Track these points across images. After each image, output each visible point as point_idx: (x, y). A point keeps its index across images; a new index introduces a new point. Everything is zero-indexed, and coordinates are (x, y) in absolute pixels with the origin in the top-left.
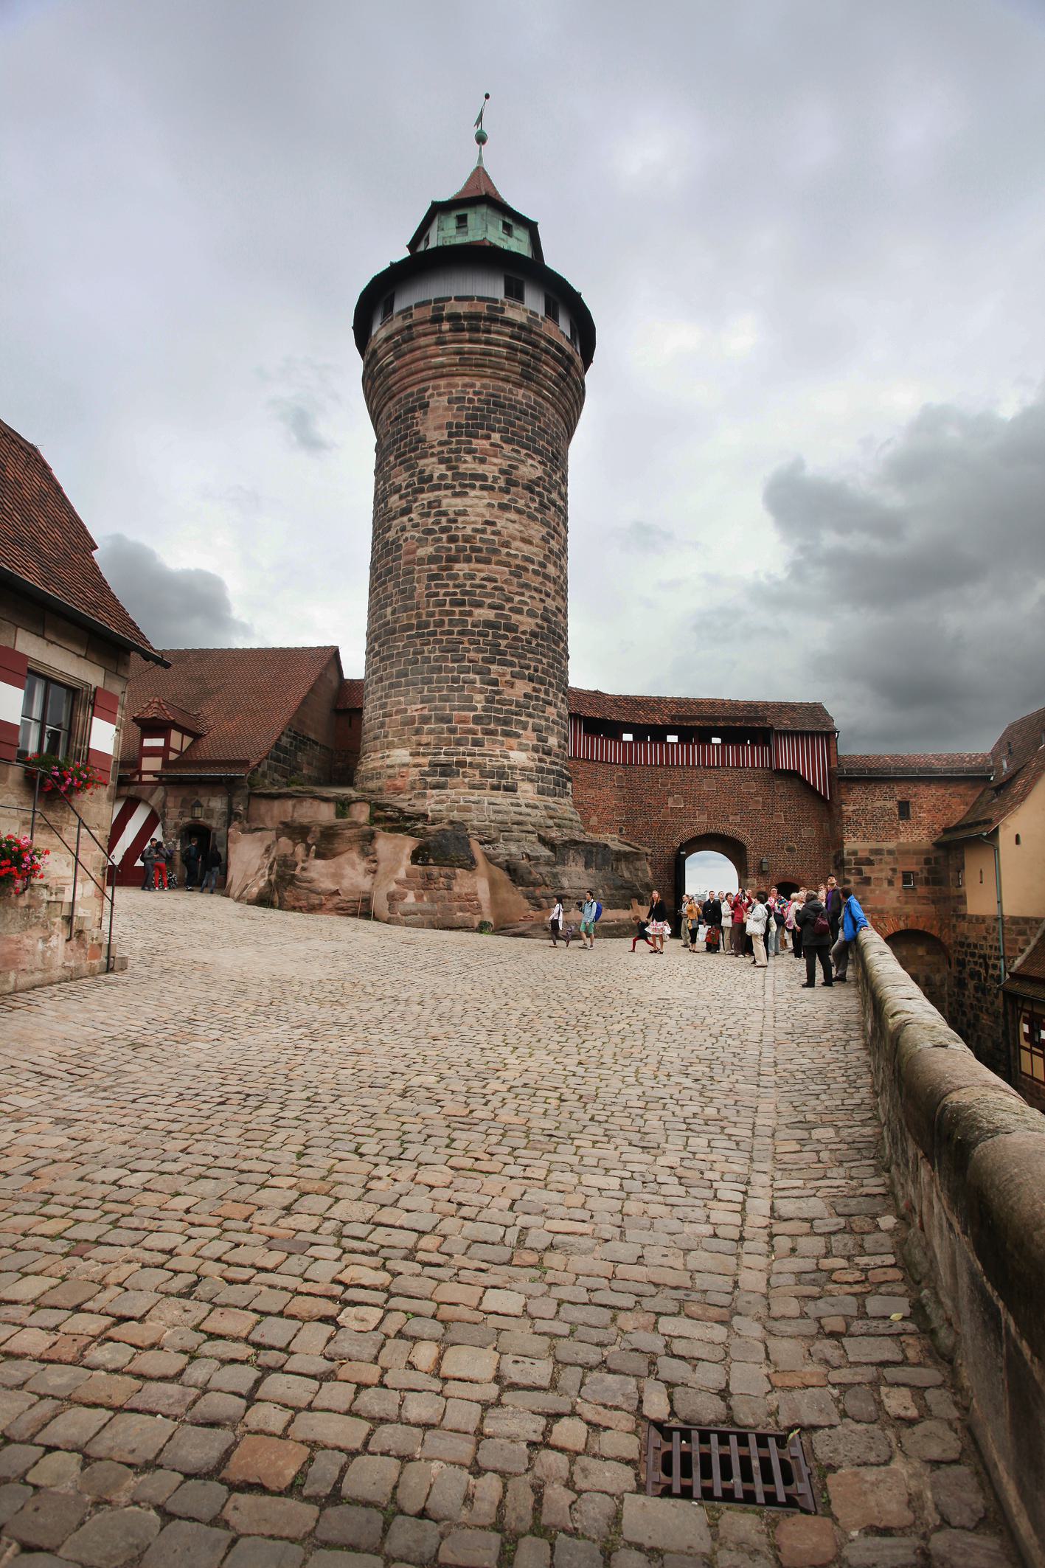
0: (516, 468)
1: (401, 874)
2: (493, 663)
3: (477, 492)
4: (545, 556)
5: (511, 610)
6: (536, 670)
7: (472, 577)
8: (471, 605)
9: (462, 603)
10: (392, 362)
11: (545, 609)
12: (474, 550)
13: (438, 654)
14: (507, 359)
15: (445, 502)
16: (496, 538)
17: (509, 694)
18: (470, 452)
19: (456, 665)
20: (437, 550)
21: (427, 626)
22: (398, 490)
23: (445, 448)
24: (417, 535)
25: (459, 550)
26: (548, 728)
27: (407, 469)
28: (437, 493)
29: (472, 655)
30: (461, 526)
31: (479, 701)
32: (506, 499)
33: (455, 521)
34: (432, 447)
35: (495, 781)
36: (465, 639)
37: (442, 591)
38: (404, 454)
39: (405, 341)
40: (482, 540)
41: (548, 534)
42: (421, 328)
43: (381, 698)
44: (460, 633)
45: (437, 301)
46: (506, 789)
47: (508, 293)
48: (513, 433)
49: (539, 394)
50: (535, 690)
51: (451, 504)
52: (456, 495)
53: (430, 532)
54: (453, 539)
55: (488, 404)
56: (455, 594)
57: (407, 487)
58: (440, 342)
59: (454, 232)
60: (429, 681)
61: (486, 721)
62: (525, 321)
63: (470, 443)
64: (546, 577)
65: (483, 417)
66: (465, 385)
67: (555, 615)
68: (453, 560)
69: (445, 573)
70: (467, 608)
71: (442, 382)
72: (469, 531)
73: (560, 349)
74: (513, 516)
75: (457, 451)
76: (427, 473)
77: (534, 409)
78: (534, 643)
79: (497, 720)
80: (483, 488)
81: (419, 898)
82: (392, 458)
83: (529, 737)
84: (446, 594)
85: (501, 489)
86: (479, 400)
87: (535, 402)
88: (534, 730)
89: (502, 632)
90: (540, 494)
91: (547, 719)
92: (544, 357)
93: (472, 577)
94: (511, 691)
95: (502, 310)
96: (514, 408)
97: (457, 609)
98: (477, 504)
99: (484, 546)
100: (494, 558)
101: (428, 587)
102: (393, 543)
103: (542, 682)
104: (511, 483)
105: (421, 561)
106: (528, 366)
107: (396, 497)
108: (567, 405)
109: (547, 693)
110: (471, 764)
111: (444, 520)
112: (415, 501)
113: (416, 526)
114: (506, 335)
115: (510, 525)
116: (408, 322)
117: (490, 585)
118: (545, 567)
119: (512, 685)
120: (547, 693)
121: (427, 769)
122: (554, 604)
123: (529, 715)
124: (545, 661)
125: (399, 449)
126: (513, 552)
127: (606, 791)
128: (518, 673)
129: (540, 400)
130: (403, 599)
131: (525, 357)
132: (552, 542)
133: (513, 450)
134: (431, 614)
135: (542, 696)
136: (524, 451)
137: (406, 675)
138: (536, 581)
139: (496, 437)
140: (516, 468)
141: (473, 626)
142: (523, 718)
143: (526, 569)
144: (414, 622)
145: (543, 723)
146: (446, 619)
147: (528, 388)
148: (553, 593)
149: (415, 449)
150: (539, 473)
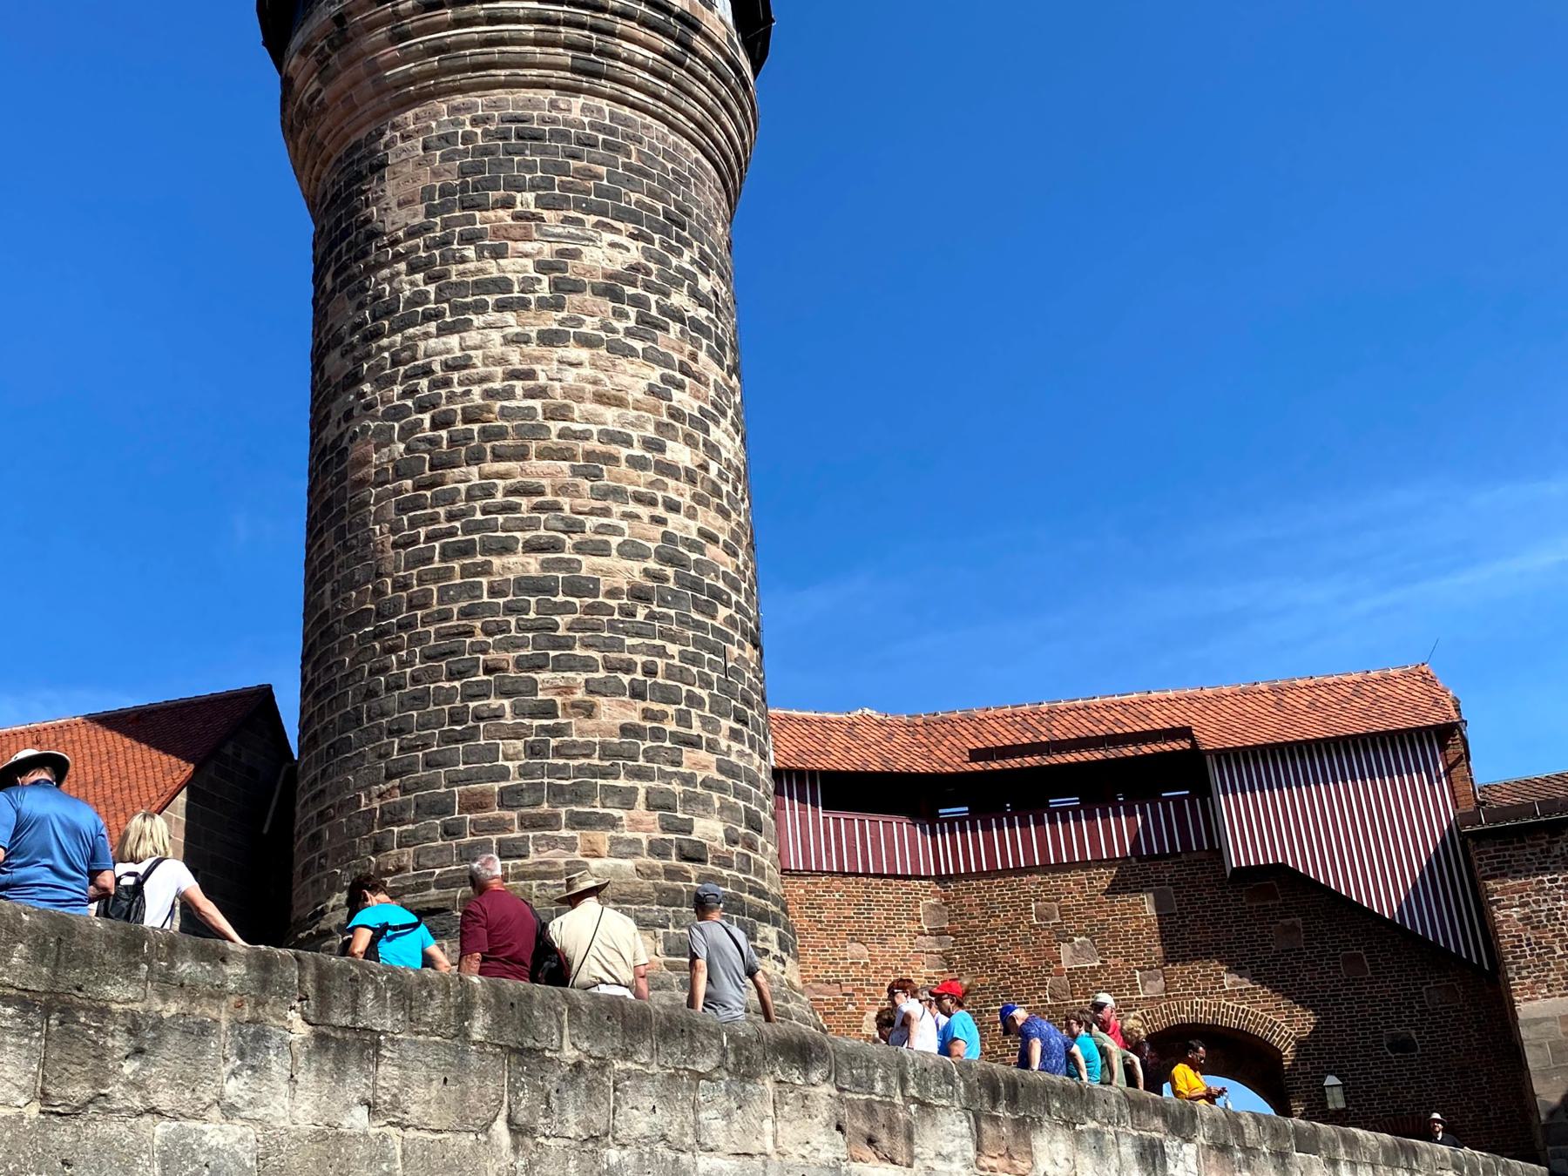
0: (576, 255)
2: (540, 667)
3: (492, 316)
4: (659, 426)
5: (578, 548)
6: (650, 671)
8: (487, 551)
9: (466, 550)
10: (319, 91)
14: (536, 43)
15: (422, 345)
16: (537, 404)
17: (580, 730)
19: (457, 684)
25: (452, 441)
26: (690, 799)
29: (493, 654)
30: (458, 390)
31: (512, 755)
32: (551, 320)
33: (447, 383)
34: (395, 242)
38: (345, 267)
39: (334, 48)
40: (505, 413)
43: (315, 780)
44: (465, 613)
48: (564, 187)
50: (647, 714)
52: (444, 330)
53: (398, 413)
55: (505, 138)
56: (451, 533)
63: (471, 220)
64: (669, 469)
65: (500, 164)
67: (700, 549)
70: (479, 558)
74: (574, 352)
75: (445, 242)
77: (613, 132)
79: (557, 793)
80: (501, 307)
83: (642, 825)
85: (543, 304)
86: (486, 133)
87: (613, 116)
88: (650, 807)
89: (560, 598)
90: (637, 301)
91: (688, 780)
92: (621, 25)
93: (488, 492)
94: (588, 724)
96: (565, 136)
100: (533, 445)
103: (669, 696)
106: (588, 49)
108: (698, 111)
109: (683, 718)
111: (424, 383)
115: (570, 375)
117: (524, 502)
118: (661, 448)
119: (589, 711)
120: (683, 718)
122: (693, 526)
126: (575, 427)
127: (901, 943)
128: (604, 682)
129: (627, 111)
131: (574, 34)
132: (676, 394)
133: (566, 220)
135: (670, 726)
138: (641, 480)
139: (526, 200)
140: (576, 255)
141: (493, 592)
142: (622, 782)
143: (612, 459)
145: (677, 787)
148: (686, 501)
150: (635, 253)
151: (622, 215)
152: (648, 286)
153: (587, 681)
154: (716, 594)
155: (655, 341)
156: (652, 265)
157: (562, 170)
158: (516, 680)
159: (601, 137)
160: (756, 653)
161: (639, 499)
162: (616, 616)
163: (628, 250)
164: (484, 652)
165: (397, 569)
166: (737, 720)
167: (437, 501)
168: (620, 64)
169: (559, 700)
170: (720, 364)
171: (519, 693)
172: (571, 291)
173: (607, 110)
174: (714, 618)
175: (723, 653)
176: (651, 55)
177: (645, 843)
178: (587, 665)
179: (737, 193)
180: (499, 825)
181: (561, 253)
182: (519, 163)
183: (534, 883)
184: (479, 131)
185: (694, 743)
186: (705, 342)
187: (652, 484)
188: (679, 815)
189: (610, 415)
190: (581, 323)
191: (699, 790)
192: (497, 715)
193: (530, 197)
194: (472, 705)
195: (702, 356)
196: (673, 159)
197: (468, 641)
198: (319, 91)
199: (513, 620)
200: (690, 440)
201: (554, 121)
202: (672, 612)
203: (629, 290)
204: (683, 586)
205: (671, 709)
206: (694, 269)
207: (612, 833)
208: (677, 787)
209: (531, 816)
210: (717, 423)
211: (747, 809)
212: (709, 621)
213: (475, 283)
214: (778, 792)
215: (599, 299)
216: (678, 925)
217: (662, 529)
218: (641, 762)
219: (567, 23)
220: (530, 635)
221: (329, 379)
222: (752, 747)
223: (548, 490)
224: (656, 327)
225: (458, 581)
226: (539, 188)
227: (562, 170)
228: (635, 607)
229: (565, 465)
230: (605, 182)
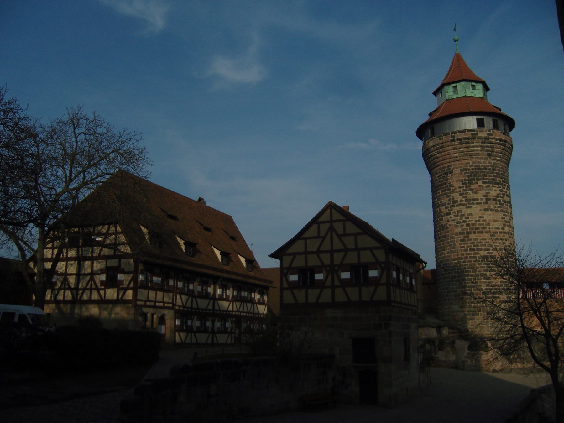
0: (489, 193)
1: (465, 354)
7: (477, 239)
9: (474, 250)
12: (476, 228)
16: (484, 223)
18: (471, 190)
19: (474, 274)
20: (462, 229)
21: (462, 259)
22: (444, 205)
23: (461, 189)
24: (454, 224)
27: (447, 197)
28: (460, 207)
29: (479, 269)
30: (470, 219)
32: (486, 206)
33: (468, 218)
34: (456, 189)
36: (477, 263)
37: (466, 246)
38: (445, 191)
40: (479, 224)
41: (504, 215)
42: (447, 144)
44: (474, 261)
45: (452, 133)
47: (478, 126)
49: (495, 160)
52: (467, 207)
56: (471, 246)
57: (448, 204)
58: (455, 149)
59: (452, 93)
62: (486, 135)
63: (470, 186)
64: (505, 233)
65: (475, 175)
66: (466, 164)
68: (468, 233)
69: (466, 239)
70: (476, 251)
71: (457, 163)
72: (473, 222)
73: (501, 140)
74: (489, 212)
75: (466, 190)
76: (455, 199)
77: (493, 166)
80: (477, 204)
81: (472, 361)
82: (440, 191)
84: (468, 247)
85: (484, 203)
87: (494, 163)
89: (490, 259)
95: (477, 134)
96: (485, 169)
97: (472, 252)
98: (476, 210)
99: (480, 227)
101: (460, 244)
102: (445, 225)
104: (487, 199)
105: (457, 234)
106: (489, 151)
107: (444, 207)
111: (464, 218)
112: (452, 210)
113: (453, 220)
114: (479, 143)
116: (441, 141)
125: (443, 188)
126: (491, 227)
129: (496, 162)
130: (451, 248)
131: (488, 148)
134: (463, 254)
136: (491, 185)
137: (455, 277)
139: (480, 183)
143: (496, 233)
144: (456, 257)
146: (468, 256)
149: (449, 189)
150: (498, 192)
157: (486, 176)
167: (468, 240)
181: (487, 193)
190: (490, 206)
203: (498, 199)
227: (486, 176)
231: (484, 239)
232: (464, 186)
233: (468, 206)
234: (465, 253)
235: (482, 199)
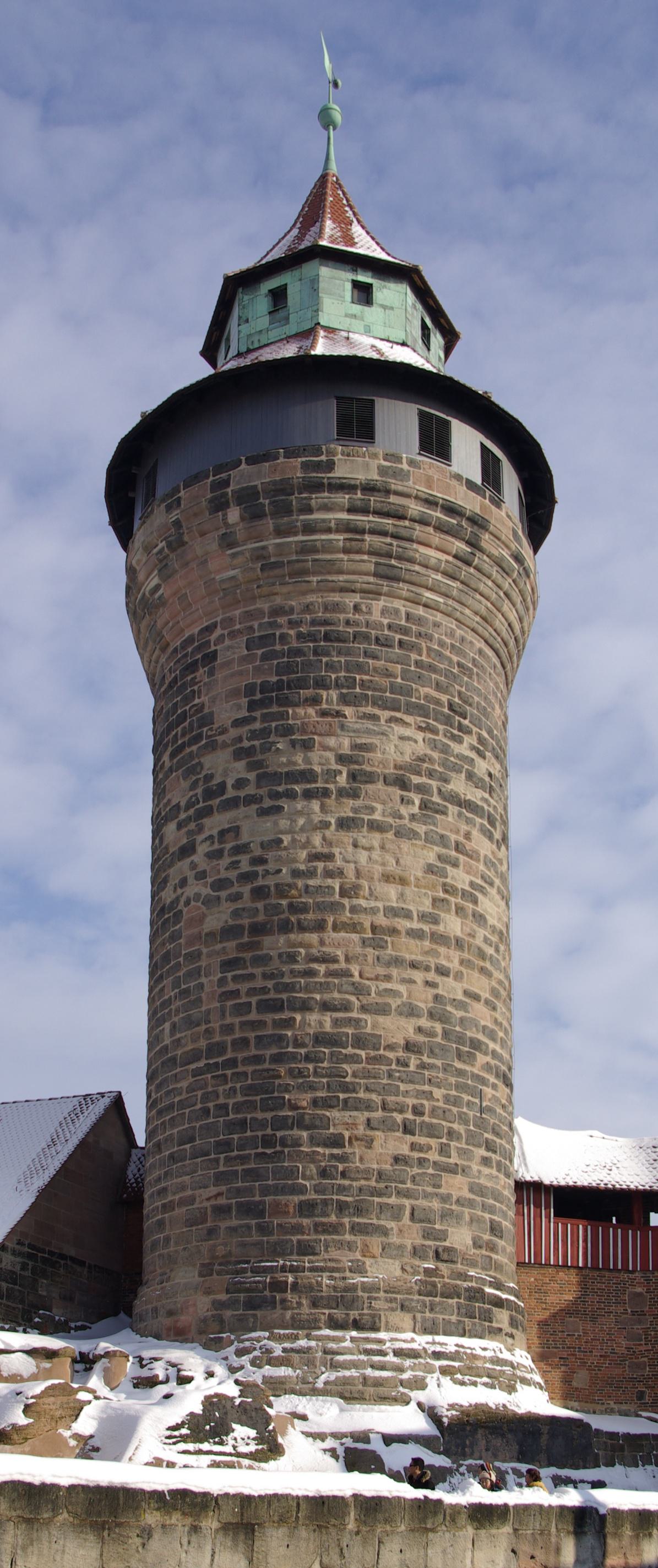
3: (300, 805)
9: (277, 1006)
11: (437, 998)
13: (240, 1098)
18: (287, 731)
19: (268, 1115)
20: (236, 914)
30: (271, 866)
32: (347, 808)
35: (338, 1313)
37: (244, 987)
46: (357, 1325)
50: (413, 1147)
51: (254, 829)
52: (263, 812)
53: (220, 884)
54: (260, 893)
55: (315, 641)
56: (264, 990)
60: (225, 1146)
61: (318, 1211)
63: (284, 716)
65: (308, 665)
68: (258, 930)
69: (248, 955)
70: (285, 1015)
74: (365, 837)
75: (265, 733)
78: (413, 1062)
79: (342, 1207)
80: (308, 795)
84: (252, 992)
85: (342, 793)
86: (300, 636)
87: (408, 616)
89: (349, 1051)
91: (445, 1199)
96: (366, 637)
97: (269, 1017)
100: (330, 920)
101: (222, 981)
103: (432, 1131)
109: (444, 1150)
110: (295, 1285)
111: (244, 860)
115: (363, 856)
117: (322, 968)
118: (435, 920)
119: (369, 1143)
120: (444, 1150)
121: (223, 1297)
123: (407, 1194)
124: (438, 1093)
129: (421, 611)
134: (228, 1029)
136: (385, 715)
141: (297, 1044)
142: (393, 1200)
143: (394, 931)
145: (436, 1205)
146: (251, 1035)
147: (389, 595)
148: (454, 965)
151: (413, 709)
152: (430, 774)
153: (368, 1120)
154: (476, 1045)
155: (435, 824)
156: (435, 755)
158: (314, 1117)
159: (398, 637)
160: (508, 1090)
161: (413, 965)
162: (394, 1067)
163: (416, 742)
164: (287, 1091)
165: (223, 1015)
166: (488, 1149)
168: (417, 568)
169: (347, 1134)
170: (490, 837)
171: (316, 1127)
172: (366, 782)
173: (403, 610)
174: (473, 1065)
175: (481, 1095)
176: (444, 557)
177: (409, 1248)
178: (369, 1107)
179: (514, 671)
180: (298, 1229)
182: (327, 664)
183: (325, 1274)
184: (292, 632)
185: (453, 1170)
186: (478, 820)
187: (427, 953)
188: (437, 1226)
189: (392, 891)
190: (372, 810)
191: (454, 1207)
192: (297, 1143)
193: (334, 694)
194: (279, 1134)
195: (475, 833)
196: (459, 652)
197: (277, 1082)
198: (157, 587)
199: (311, 1066)
200: (460, 910)
201: (356, 624)
202: (439, 1063)
203: (416, 780)
204: (449, 1040)
205: (433, 1142)
206: (473, 755)
207: (384, 1239)
208: (436, 1205)
209: (323, 1224)
210: (485, 894)
211: (492, 1221)
212: (468, 1068)
213: (287, 773)
214: (519, 1201)
215: (390, 789)
216: (432, 1310)
217: (435, 991)
218: (409, 1185)
219: (373, 532)
220: (325, 1080)
221: (167, 848)
222: (499, 1170)
223: (342, 958)
224: (437, 812)
225: (270, 1032)
226: (343, 687)
228: (409, 1058)
229: (355, 937)
230: (399, 680)
231: (325, 959)
232: (258, 714)
233: (268, 803)
234: (237, 1020)
235: (332, 775)
